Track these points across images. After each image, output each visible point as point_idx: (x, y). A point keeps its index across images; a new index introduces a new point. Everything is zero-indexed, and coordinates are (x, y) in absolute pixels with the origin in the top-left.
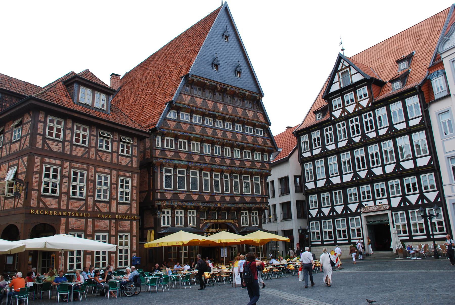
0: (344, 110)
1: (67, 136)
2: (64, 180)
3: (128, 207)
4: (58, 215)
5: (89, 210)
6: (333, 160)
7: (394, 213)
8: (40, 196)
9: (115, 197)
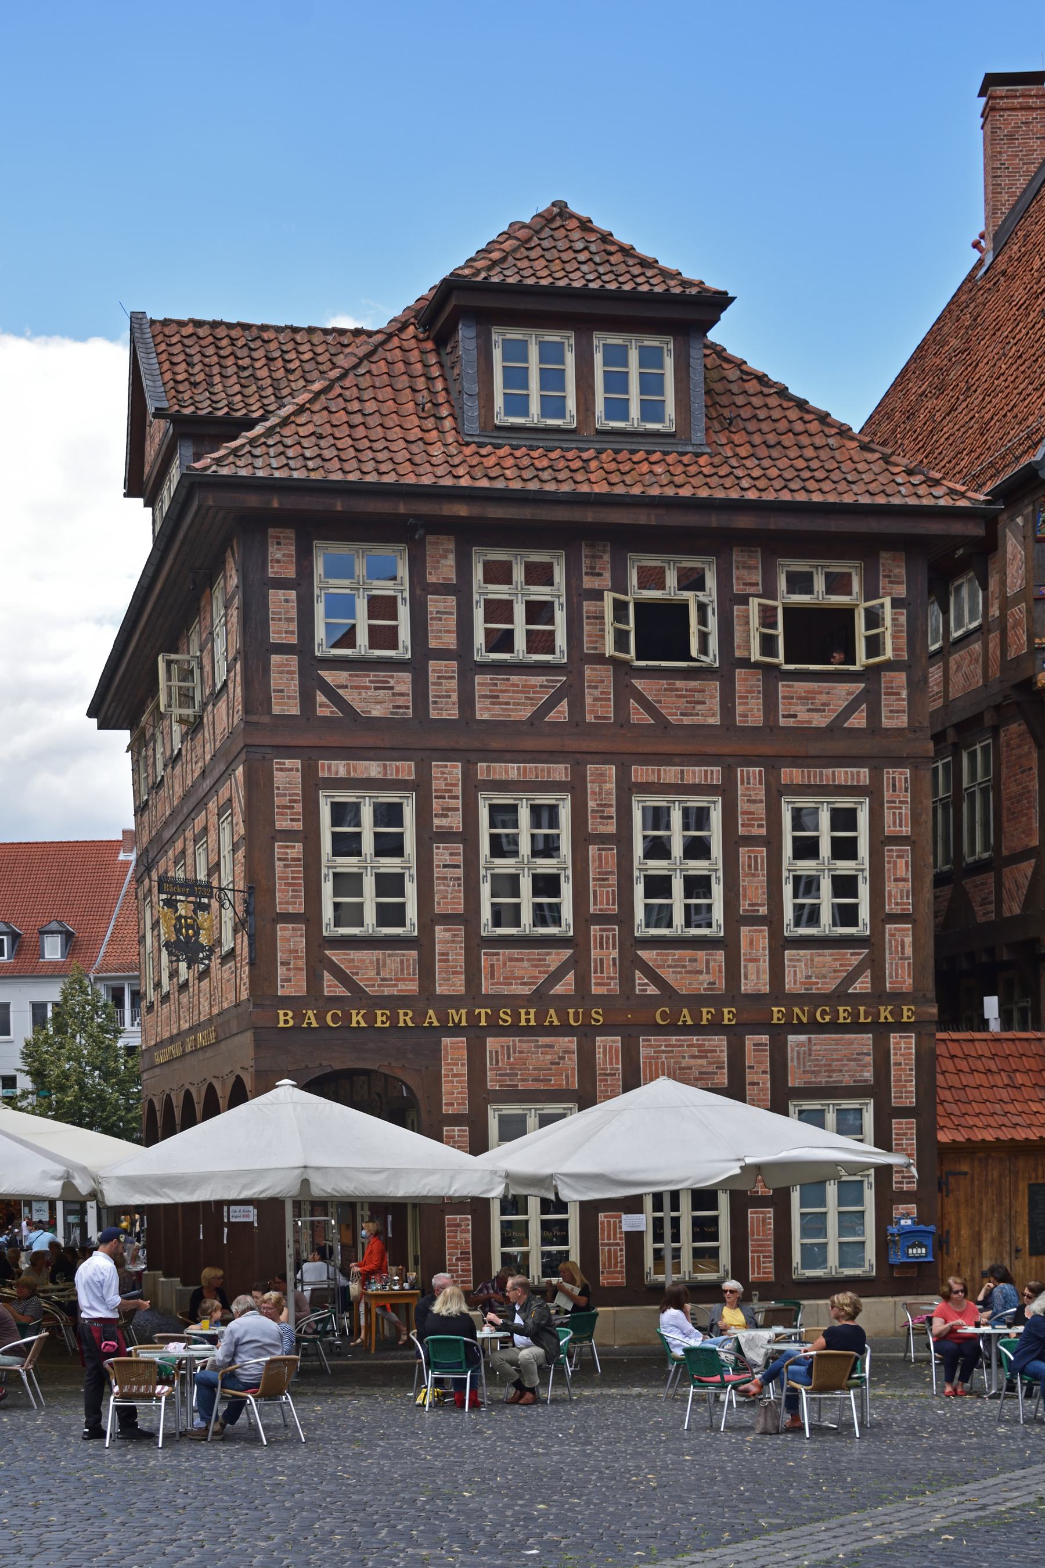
1: (433, 626)
2: (442, 854)
3: (853, 958)
4: (419, 1027)
5: (595, 990)
8: (318, 944)
9: (763, 910)
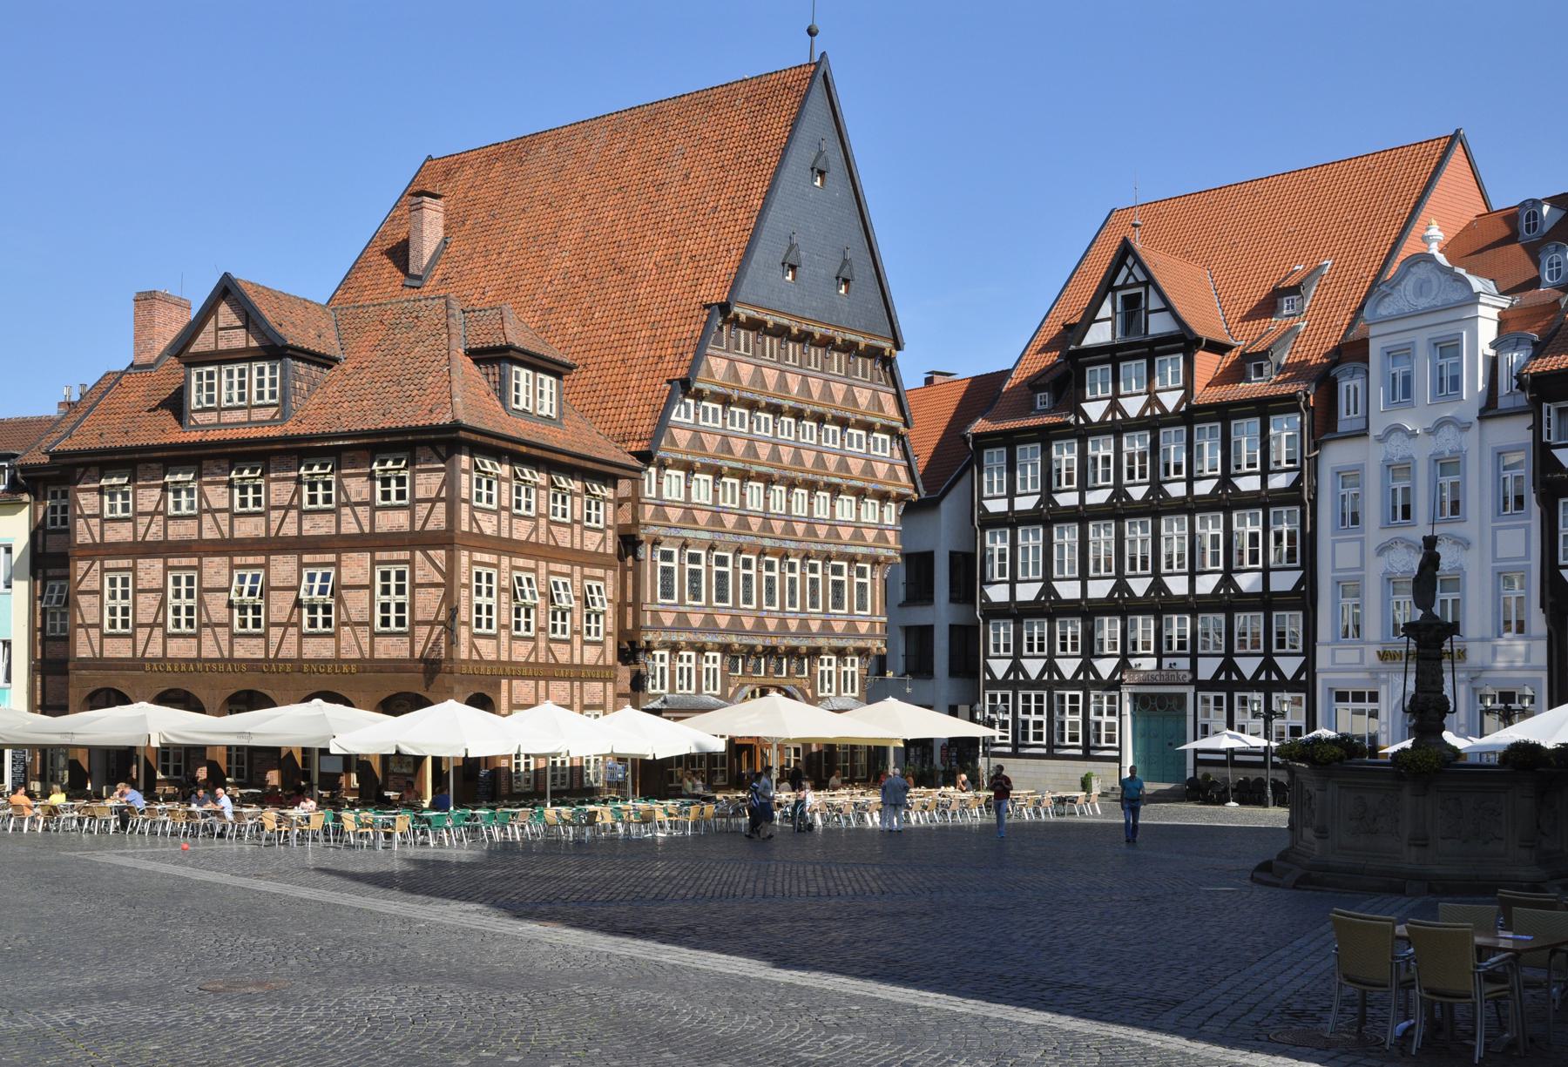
0: (1114, 406)
3: (599, 649)
6: (1067, 537)
7: (1200, 694)
